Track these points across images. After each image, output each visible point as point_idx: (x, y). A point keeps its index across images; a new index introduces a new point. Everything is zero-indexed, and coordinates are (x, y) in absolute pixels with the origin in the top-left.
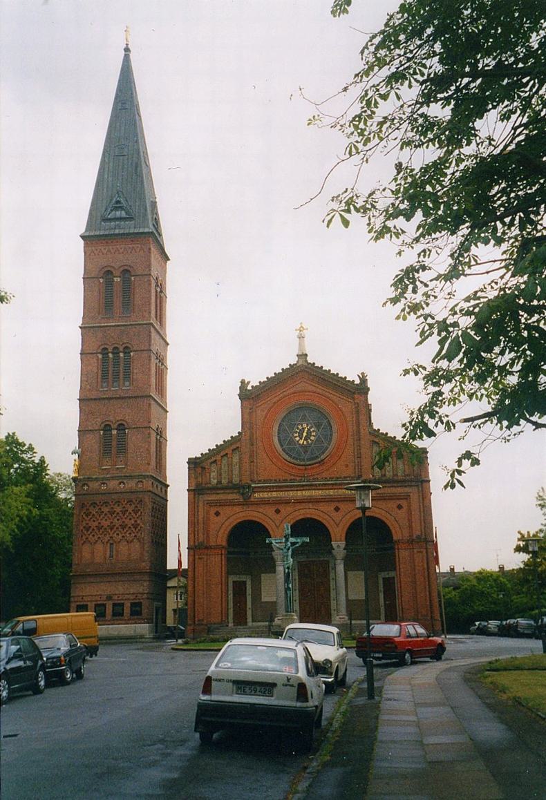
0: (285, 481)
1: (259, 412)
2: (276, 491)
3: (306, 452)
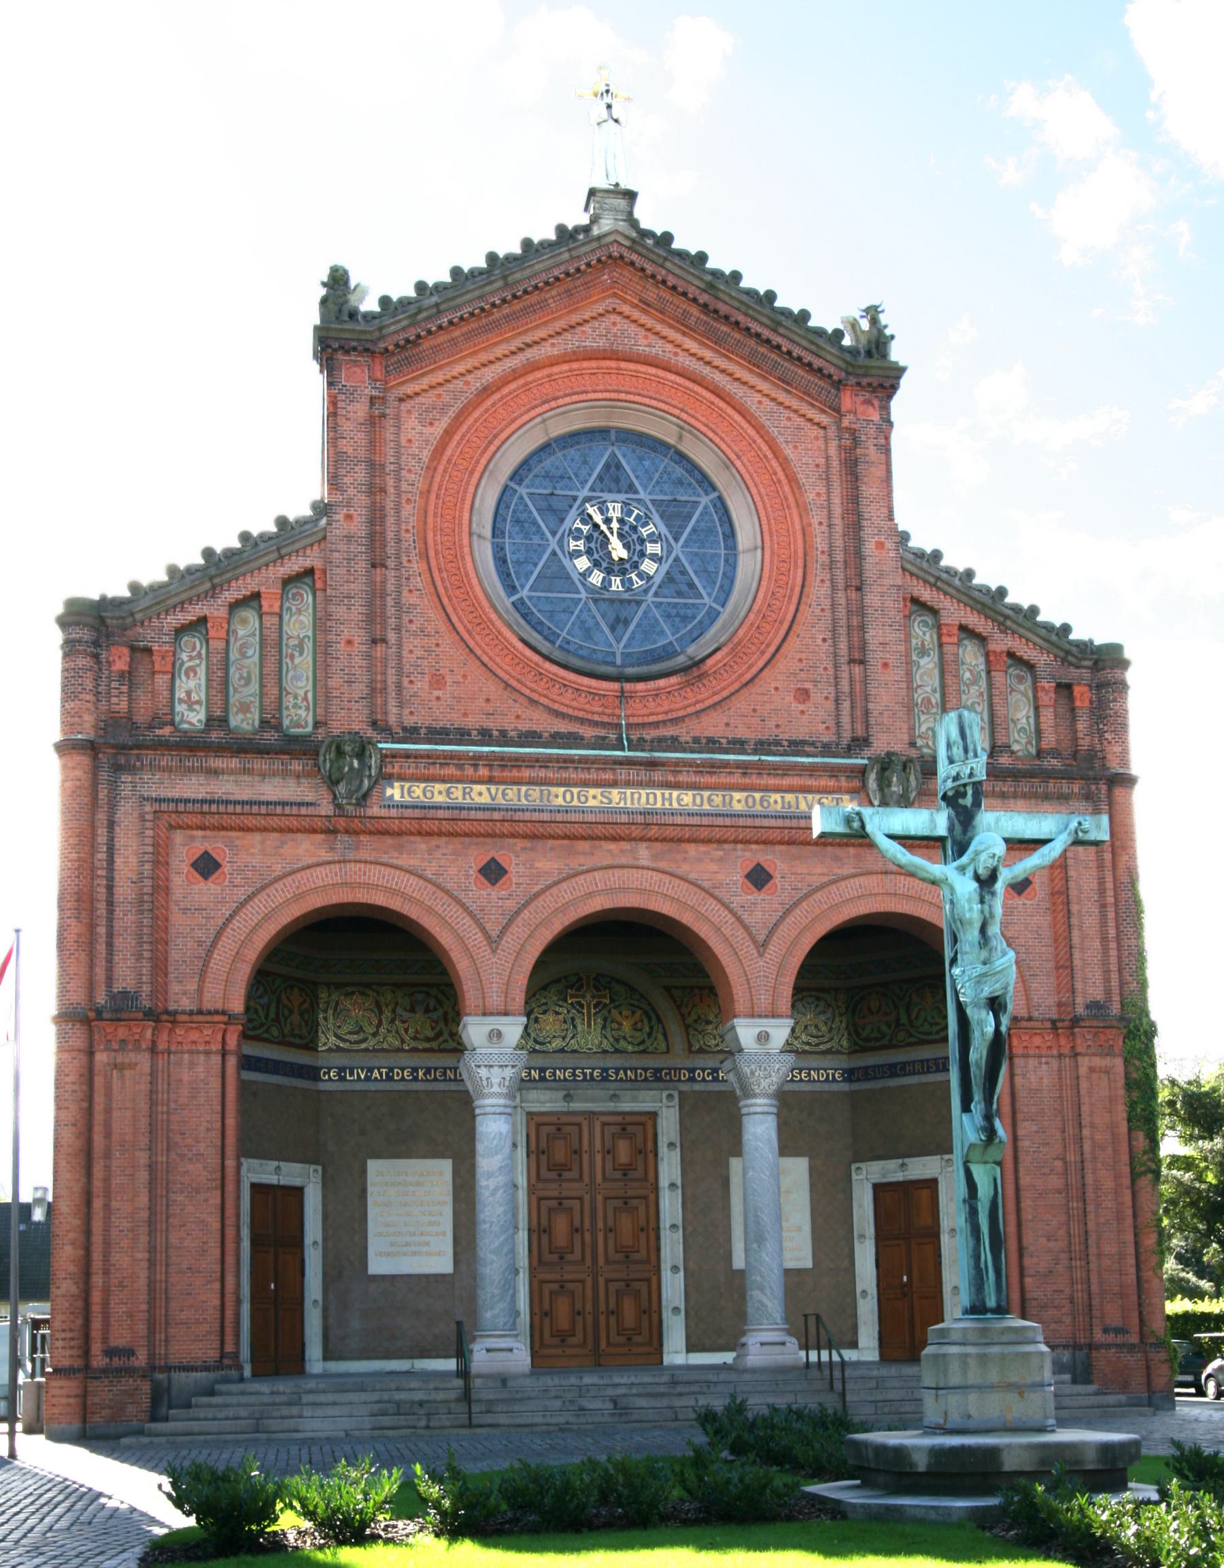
0: (530, 738)
1: (412, 427)
2: (490, 781)
3: (618, 623)
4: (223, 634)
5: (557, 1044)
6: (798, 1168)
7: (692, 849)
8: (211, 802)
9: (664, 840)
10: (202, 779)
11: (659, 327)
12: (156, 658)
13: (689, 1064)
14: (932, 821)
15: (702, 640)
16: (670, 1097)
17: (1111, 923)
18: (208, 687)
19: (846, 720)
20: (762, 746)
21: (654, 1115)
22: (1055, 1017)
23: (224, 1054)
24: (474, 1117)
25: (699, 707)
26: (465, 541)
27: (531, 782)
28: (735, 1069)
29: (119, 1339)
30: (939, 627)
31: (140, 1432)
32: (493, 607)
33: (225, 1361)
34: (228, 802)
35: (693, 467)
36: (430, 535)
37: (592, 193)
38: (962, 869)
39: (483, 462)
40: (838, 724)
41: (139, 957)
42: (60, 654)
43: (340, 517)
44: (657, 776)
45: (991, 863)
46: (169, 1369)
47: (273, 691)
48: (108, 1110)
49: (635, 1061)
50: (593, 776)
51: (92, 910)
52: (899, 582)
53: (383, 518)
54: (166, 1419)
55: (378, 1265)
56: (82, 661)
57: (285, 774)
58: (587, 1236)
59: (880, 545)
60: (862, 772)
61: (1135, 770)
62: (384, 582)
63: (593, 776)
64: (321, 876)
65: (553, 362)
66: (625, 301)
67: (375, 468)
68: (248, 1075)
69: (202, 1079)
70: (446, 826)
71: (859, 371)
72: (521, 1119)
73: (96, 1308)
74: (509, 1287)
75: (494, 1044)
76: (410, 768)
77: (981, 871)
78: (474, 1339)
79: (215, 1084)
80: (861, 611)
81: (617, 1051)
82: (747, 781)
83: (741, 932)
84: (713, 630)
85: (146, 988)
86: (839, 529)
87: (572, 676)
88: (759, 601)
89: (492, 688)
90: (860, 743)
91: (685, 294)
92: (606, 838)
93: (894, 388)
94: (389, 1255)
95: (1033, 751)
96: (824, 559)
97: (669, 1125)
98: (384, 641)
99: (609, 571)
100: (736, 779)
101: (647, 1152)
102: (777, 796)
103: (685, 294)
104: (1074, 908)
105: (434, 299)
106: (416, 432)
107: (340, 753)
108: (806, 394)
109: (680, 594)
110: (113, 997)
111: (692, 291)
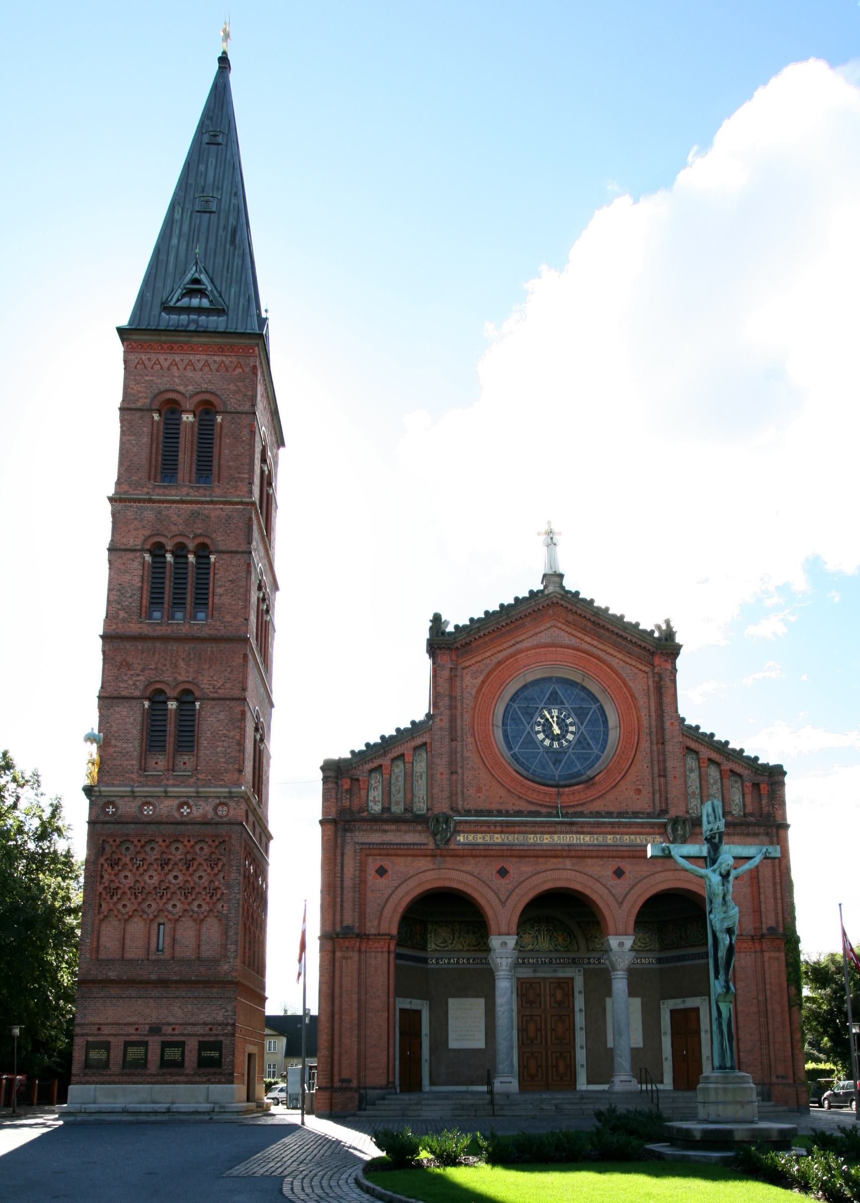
0: (519, 813)
1: (468, 680)
2: (502, 832)
3: (556, 762)
4: (388, 772)
5: (530, 947)
6: (637, 1002)
7: (589, 861)
8: (384, 844)
9: (578, 857)
10: (380, 834)
11: (574, 632)
12: (361, 783)
13: (588, 956)
14: (701, 849)
15: (593, 768)
16: (579, 971)
17: (779, 891)
18: (383, 795)
19: (657, 802)
20: (620, 815)
21: (572, 979)
22: (753, 934)
23: (389, 953)
24: (494, 980)
25: (592, 798)
26: (491, 728)
27: (519, 833)
28: (608, 958)
29: (346, 1075)
30: (699, 759)
31: (354, 1115)
32: (502, 756)
33: (389, 1085)
34: (391, 844)
35: (589, 693)
36: (476, 726)
37: (545, 576)
38: (714, 871)
39: (498, 694)
40: (654, 804)
41: (354, 911)
42: (321, 782)
43: (437, 720)
44: (574, 829)
45: (727, 868)
46: (366, 1088)
47: (409, 796)
48: (341, 977)
49: (564, 955)
50: (546, 829)
51: (335, 891)
52: (681, 740)
53: (456, 720)
54: (365, 1110)
55: (453, 1044)
56: (331, 785)
57: (415, 831)
58: (543, 1032)
59: (672, 724)
60: (665, 825)
61: (789, 822)
62: (456, 748)
63: (546, 829)
64: (430, 875)
65: (528, 649)
66: (559, 621)
67: (452, 698)
68: (399, 962)
69: (380, 963)
70: (483, 853)
71: (662, 649)
72: (514, 980)
73: (336, 1062)
74: (510, 1054)
75: (503, 948)
76: (467, 827)
77: (723, 871)
78: (495, 1077)
79: (385, 966)
80: (663, 753)
81: (556, 950)
82: (613, 830)
83: (611, 898)
84: (598, 764)
85: (357, 924)
86: (654, 717)
87: (536, 786)
88: (618, 751)
89: (502, 792)
90: (663, 812)
91: (585, 617)
92: (552, 857)
93: (678, 654)
94: (457, 1040)
95: (742, 814)
96: (647, 731)
97: (579, 983)
98: (456, 773)
99: (553, 740)
100: (609, 829)
101: (569, 995)
102: (627, 837)
103: (585, 617)
104: (761, 885)
105: (477, 625)
106: (470, 682)
107: (438, 822)
108: (639, 658)
109: (584, 748)
110: (343, 928)
111: (588, 616)
